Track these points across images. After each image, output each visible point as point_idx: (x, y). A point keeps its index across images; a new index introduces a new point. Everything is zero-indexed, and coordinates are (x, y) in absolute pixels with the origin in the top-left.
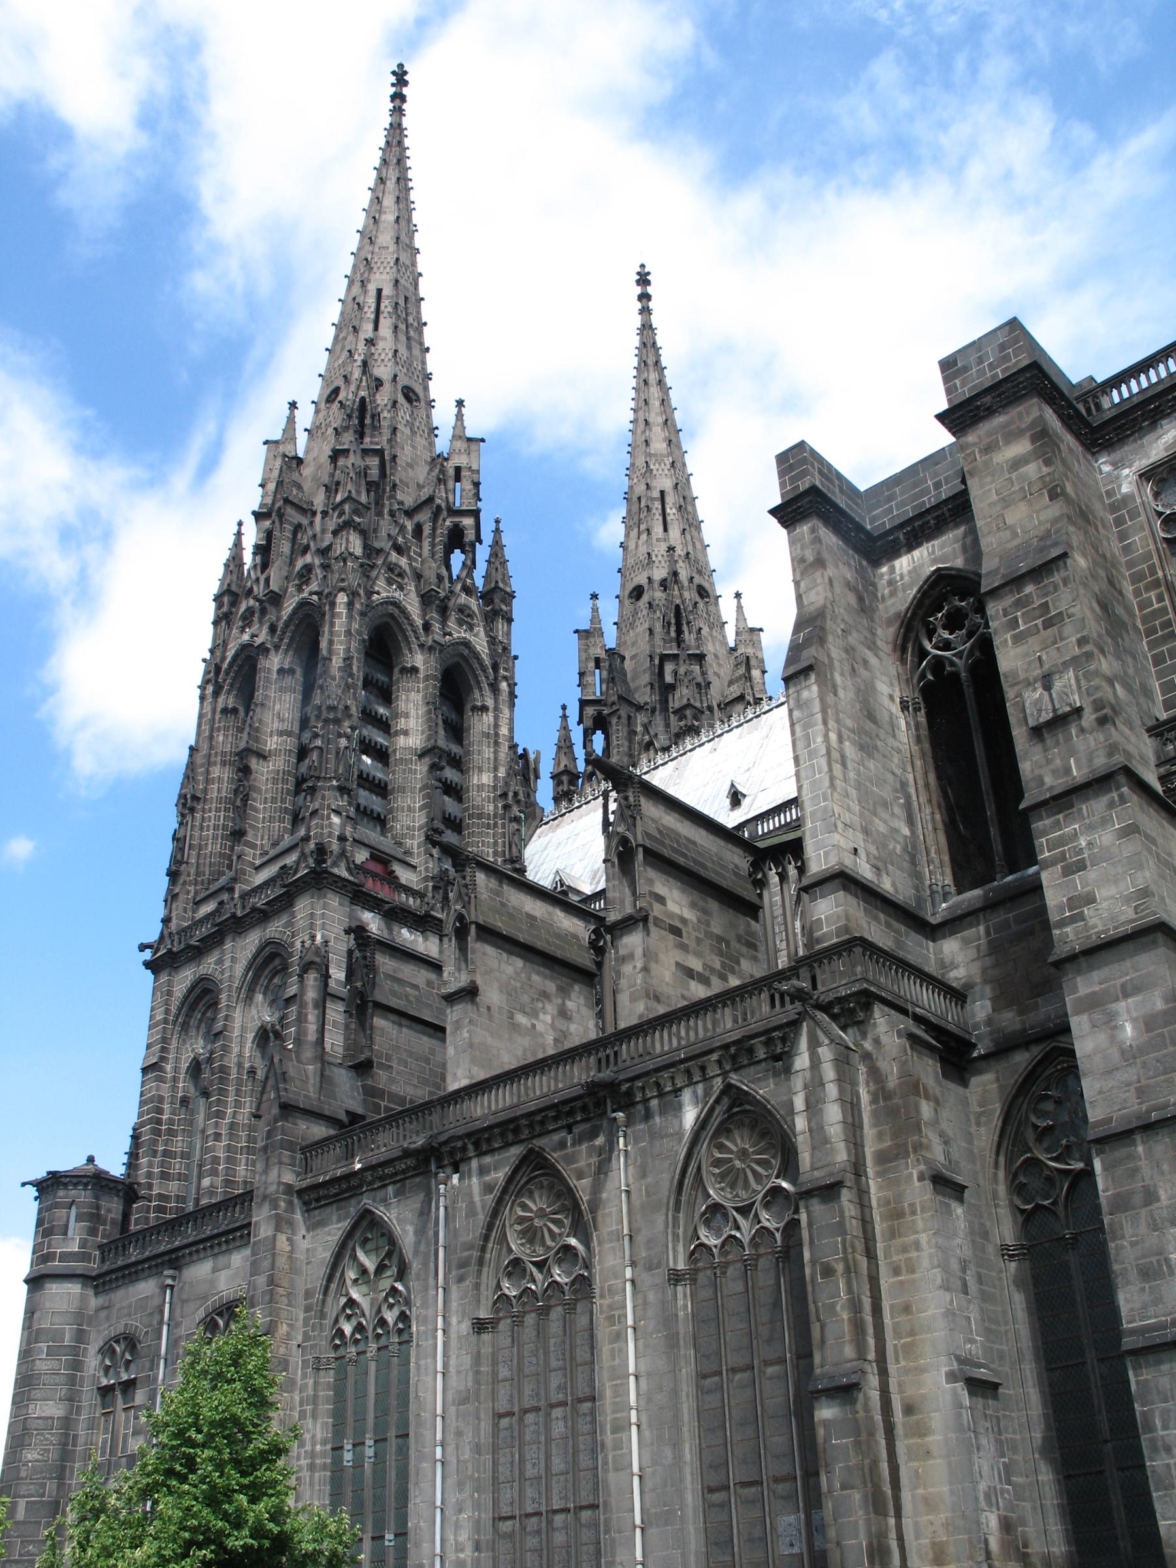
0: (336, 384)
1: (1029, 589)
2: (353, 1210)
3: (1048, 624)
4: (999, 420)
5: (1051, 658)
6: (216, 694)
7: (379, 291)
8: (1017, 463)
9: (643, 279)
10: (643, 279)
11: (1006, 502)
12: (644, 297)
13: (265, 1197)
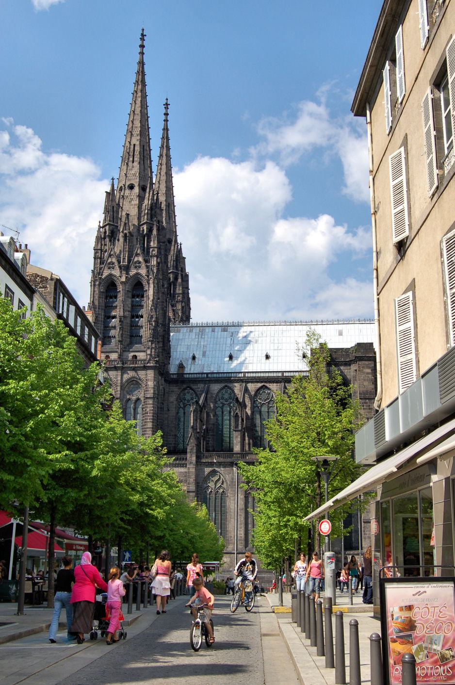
0: (132, 182)
1: (367, 401)
2: (213, 469)
3: (370, 409)
4: (367, 363)
5: (369, 416)
6: (99, 285)
7: (144, 146)
8: (368, 373)
9: (167, 105)
10: (167, 105)
11: (365, 380)
12: (166, 114)
13: (191, 463)
